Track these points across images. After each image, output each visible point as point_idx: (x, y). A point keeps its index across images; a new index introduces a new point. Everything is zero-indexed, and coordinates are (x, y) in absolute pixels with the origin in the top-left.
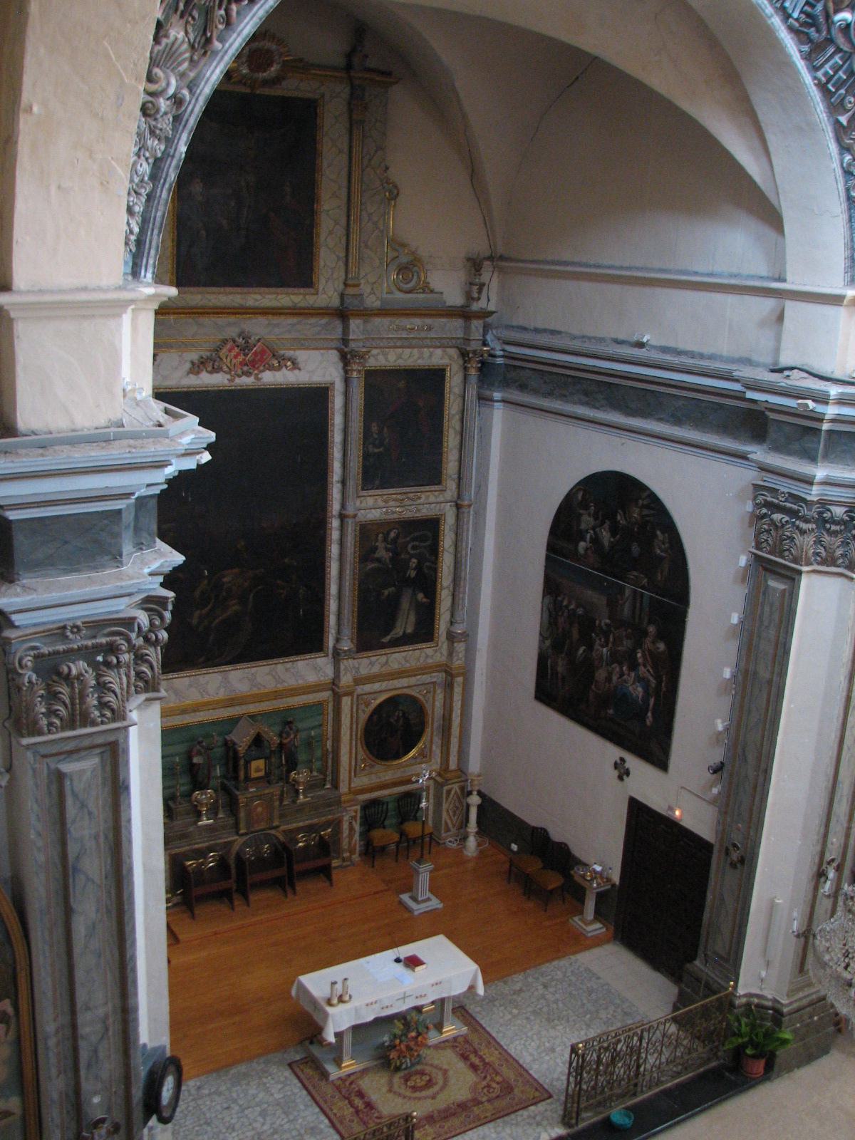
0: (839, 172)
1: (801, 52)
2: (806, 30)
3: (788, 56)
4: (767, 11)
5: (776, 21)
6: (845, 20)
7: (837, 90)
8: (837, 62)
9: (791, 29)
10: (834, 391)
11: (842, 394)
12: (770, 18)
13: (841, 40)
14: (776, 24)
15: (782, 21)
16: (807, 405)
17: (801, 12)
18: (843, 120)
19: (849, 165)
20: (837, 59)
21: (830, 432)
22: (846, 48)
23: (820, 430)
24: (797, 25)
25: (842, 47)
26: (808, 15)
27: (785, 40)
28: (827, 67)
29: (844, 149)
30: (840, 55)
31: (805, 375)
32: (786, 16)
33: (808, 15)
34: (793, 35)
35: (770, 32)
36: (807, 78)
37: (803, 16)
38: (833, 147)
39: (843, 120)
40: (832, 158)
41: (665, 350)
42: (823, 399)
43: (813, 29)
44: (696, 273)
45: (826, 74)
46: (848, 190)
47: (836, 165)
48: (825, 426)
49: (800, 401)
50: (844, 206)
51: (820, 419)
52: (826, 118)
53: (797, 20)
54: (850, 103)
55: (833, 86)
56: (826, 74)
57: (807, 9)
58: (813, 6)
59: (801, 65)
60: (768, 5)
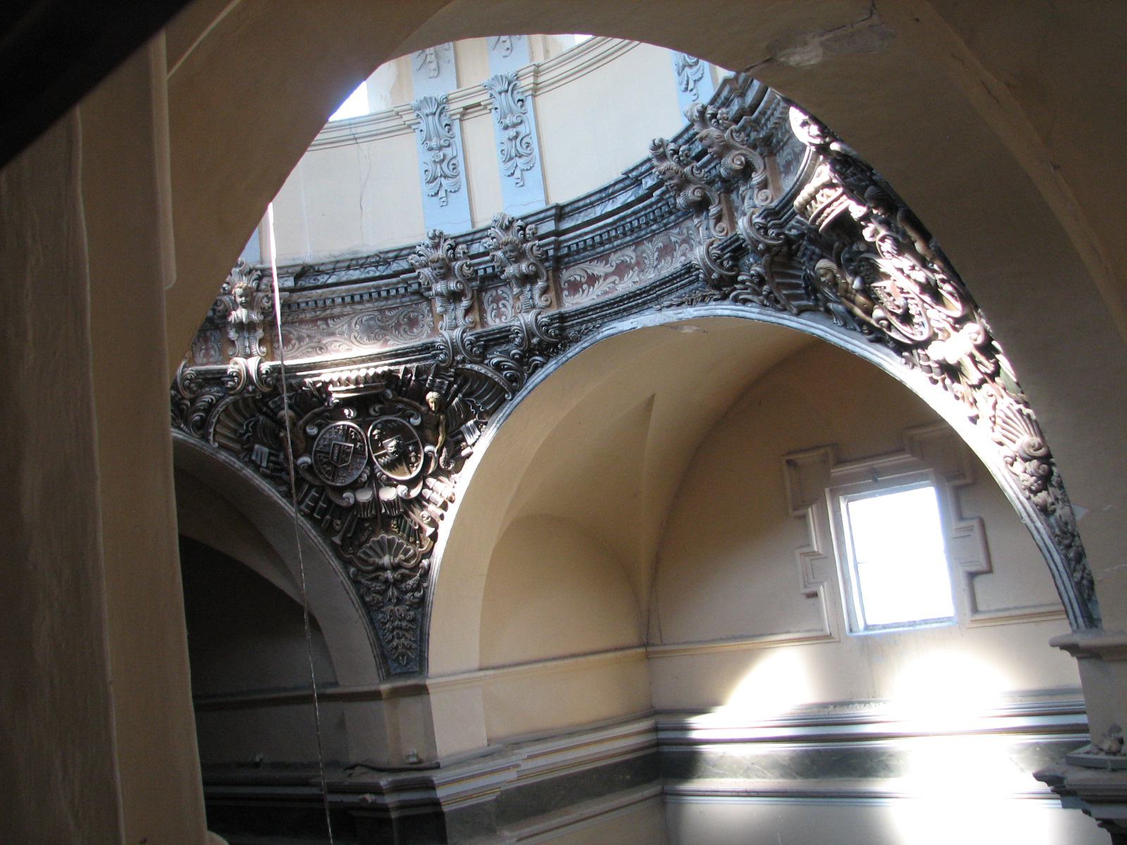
0: (348, 583)
1: (280, 492)
2: (279, 475)
3: (269, 497)
4: (236, 466)
5: (248, 472)
6: (306, 463)
7: (323, 517)
8: (314, 495)
9: (265, 476)
10: (384, 781)
11: (394, 782)
12: (241, 471)
13: (309, 478)
14: (248, 475)
15: (254, 471)
16: (365, 800)
17: (268, 462)
18: (337, 540)
19: (355, 575)
20: (313, 493)
21: (400, 819)
22: (317, 483)
23: (390, 820)
24: (269, 472)
25: (313, 483)
26: (276, 463)
27: (262, 486)
28: (307, 501)
29: (346, 563)
30: (314, 489)
31: (365, 770)
32: (257, 468)
33: (276, 463)
34: (268, 480)
35: (246, 482)
36: (291, 510)
37: (271, 465)
38: (335, 564)
39: (337, 540)
40: (336, 573)
41: (277, 766)
42: (378, 791)
43: (283, 473)
44: (285, 689)
45: (307, 506)
46: (362, 597)
47: (342, 577)
48: (394, 815)
49: (361, 797)
50: (362, 611)
51: (385, 809)
52: (321, 541)
53: (267, 468)
54: (337, 525)
55: (318, 514)
56: (307, 506)
57: (273, 458)
58: (277, 456)
59: (283, 502)
60: (236, 461)
